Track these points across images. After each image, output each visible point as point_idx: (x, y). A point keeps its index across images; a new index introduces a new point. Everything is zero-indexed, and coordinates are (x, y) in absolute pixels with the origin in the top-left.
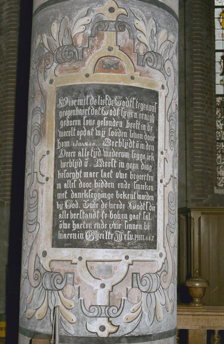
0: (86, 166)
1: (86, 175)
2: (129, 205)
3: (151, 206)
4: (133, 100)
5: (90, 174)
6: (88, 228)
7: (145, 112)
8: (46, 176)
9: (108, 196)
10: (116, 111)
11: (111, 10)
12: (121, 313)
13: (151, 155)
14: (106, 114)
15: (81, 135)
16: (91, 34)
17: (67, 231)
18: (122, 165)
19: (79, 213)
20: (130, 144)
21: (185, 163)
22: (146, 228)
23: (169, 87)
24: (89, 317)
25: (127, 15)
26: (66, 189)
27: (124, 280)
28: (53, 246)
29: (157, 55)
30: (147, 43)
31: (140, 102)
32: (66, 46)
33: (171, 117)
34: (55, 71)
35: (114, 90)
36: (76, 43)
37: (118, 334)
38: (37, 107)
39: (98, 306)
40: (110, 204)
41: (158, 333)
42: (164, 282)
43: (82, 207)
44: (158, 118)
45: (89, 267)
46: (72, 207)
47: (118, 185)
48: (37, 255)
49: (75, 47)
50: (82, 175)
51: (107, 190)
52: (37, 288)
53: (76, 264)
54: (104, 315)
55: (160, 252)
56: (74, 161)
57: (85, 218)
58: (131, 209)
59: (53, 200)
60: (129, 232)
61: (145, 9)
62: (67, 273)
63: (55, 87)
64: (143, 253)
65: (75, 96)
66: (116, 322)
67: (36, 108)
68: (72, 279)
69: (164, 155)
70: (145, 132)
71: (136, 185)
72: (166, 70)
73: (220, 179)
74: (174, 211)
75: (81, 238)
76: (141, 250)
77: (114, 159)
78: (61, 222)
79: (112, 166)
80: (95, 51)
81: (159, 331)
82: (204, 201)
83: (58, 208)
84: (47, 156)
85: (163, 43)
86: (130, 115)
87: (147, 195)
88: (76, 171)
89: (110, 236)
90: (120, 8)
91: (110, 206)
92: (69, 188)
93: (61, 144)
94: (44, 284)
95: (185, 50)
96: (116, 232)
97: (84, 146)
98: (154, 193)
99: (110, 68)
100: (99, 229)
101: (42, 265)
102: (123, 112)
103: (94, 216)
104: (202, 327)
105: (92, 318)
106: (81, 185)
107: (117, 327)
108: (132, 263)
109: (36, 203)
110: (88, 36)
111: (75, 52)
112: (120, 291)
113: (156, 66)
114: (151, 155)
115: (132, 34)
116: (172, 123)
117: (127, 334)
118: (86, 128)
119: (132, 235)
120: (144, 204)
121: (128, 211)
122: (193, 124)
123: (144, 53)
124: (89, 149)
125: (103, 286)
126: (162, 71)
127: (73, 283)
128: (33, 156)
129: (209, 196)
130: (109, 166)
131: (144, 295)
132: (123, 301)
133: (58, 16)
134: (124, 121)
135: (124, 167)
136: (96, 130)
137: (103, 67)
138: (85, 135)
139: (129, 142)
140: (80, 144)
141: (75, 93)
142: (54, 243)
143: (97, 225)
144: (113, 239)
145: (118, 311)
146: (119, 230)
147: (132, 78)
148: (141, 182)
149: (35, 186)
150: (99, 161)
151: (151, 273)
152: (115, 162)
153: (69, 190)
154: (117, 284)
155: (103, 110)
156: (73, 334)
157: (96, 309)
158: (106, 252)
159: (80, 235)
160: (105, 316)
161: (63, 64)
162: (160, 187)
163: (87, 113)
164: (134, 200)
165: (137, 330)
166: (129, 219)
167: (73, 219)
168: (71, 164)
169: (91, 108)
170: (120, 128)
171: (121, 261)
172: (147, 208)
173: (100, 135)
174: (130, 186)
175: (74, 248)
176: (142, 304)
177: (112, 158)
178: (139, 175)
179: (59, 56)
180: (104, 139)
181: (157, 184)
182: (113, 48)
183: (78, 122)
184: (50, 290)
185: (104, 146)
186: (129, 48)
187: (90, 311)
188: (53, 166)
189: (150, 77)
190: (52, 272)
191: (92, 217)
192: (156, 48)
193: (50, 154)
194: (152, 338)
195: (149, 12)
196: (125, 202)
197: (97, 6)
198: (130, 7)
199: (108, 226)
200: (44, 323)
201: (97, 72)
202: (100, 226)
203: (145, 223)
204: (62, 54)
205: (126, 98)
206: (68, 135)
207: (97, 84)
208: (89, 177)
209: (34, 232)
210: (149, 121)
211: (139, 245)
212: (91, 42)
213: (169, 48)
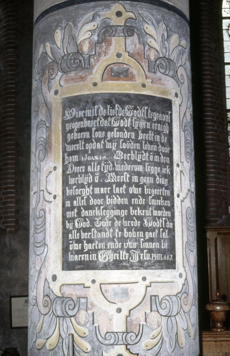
0: (97, 181)
1: (97, 190)
2: (144, 222)
3: (168, 223)
4: (145, 110)
6: (101, 247)
7: (159, 122)
8: (54, 193)
9: (122, 213)
10: (128, 121)
11: (119, 14)
13: (166, 168)
14: (116, 125)
15: (90, 148)
16: (98, 40)
17: (78, 252)
18: (135, 179)
19: (91, 232)
20: (144, 156)
23: (183, 95)
25: (135, 18)
26: (76, 207)
28: (63, 269)
29: (169, 60)
30: (158, 49)
31: (153, 111)
32: (72, 54)
33: (186, 128)
35: (124, 99)
36: (82, 50)
38: (42, 121)
39: (114, 332)
40: (124, 221)
42: (185, 305)
43: (93, 225)
45: (103, 290)
46: (83, 226)
48: (46, 279)
50: (93, 191)
51: (120, 207)
52: (47, 316)
53: (89, 287)
54: (122, 343)
56: (83, 176)
57: (97, 237)
58: (147, 226)
59: (62, 220)
61: (154, 12)
62: (80, 298)
63: (60, 98)
64: (161, 274)
65: (82, 107)
67: (40, 122)
68: (85, 304)
69: (180, 168)
71: (151, 200)
72: (179, 77)
74: (193, 228)
75: (93, 259)
76: (160, 271)
77: (126, 173)
79: (125, 181)
80: (103, 58)
82: (218, 222)
83: (67, 228)
84: (54, 172)
85: (174, 48)
86: (143, 126)
87: (163, 211)
88: (87, 187)
89: (125, 256)
90: (128, 11)
91: (124, 223)
93: (69, 158)
94: (54, 311)
96: (132, 252)
97: (93, 159)
98: (171, 209)
99: (119, 76)
101: (52, 291)
103: (108, 234)
105: (109, 346)
106: (92, 202)
108: (150, 285)
109: (43, 224)
110: (94, 42)
111: (82, 60)
112: (138, 316)
113: (169, 73)
114: (166, 168)
115: (141, 39)
116: (187, 134)
119: (149, 255)
120: (161, 220)
121: (143, 229)
123: (155, 59)
124: (99, 163)
125: (119, 310)
127: (87, 309)
129: (224, 216)
130: (122, 181)
131: (164, 319)
132: (141, 326)
133: (61, 23)
135: (137, 181)
136: (107, 142)
137: (112, 75)
138: (94, 148)
139: (142, 154)
140: (89, 158)
141: (82, 104)
143: (110, 245)
144: (129, 259)
145: (136, 337)
147: (144, 86)
148: (157, 197)
149: (42, 205)
150: (111, 175)
151: (170, 295)
153: (79, 208)
154: (134, 308)
155: (113, 121)
157: (113, 336)
158: (122, 273)
160: (123, 343)
161: (69, 73)
162: (177, 202)
163: (96, 124)
164: (150, 216)
167: (84, 239)
168: (81, 180)
169: (101, 119)
170: (132, 140)
171: (137, 283)
172: (164, 224)
173: (111, 147)
174: (145, 201)
175: (87, 270)
176: (163, 330)
177: (124, 171)
178: (154, 189)
179: (64, 65)
180: (115, 152)
181: (173, 199)
182: (121, 54)
183: (87, 135)
184: (62, 317)
185: (115, 160)
186: (138, 54)
187: (105, 338)
189: (162, 84)
190: (63, 297)
191: (105, 236)
192: (167, 54)
193: (57, 170)
195: (159, 15)
196: (140, 218)
197: (103, 10)
198: (139, 10)
199: (122, 245)
201: (106, 80)
202: (114, 245)
203: (162, 241)
204: (67, 63)
205: (138, 107)
206: (76, 148)
207: (106, 93)
208: (100, 193)
209: (42, 255)
210: (163, 131)
211: (157, 265)
212: (98, 49)
213: (181, 53)
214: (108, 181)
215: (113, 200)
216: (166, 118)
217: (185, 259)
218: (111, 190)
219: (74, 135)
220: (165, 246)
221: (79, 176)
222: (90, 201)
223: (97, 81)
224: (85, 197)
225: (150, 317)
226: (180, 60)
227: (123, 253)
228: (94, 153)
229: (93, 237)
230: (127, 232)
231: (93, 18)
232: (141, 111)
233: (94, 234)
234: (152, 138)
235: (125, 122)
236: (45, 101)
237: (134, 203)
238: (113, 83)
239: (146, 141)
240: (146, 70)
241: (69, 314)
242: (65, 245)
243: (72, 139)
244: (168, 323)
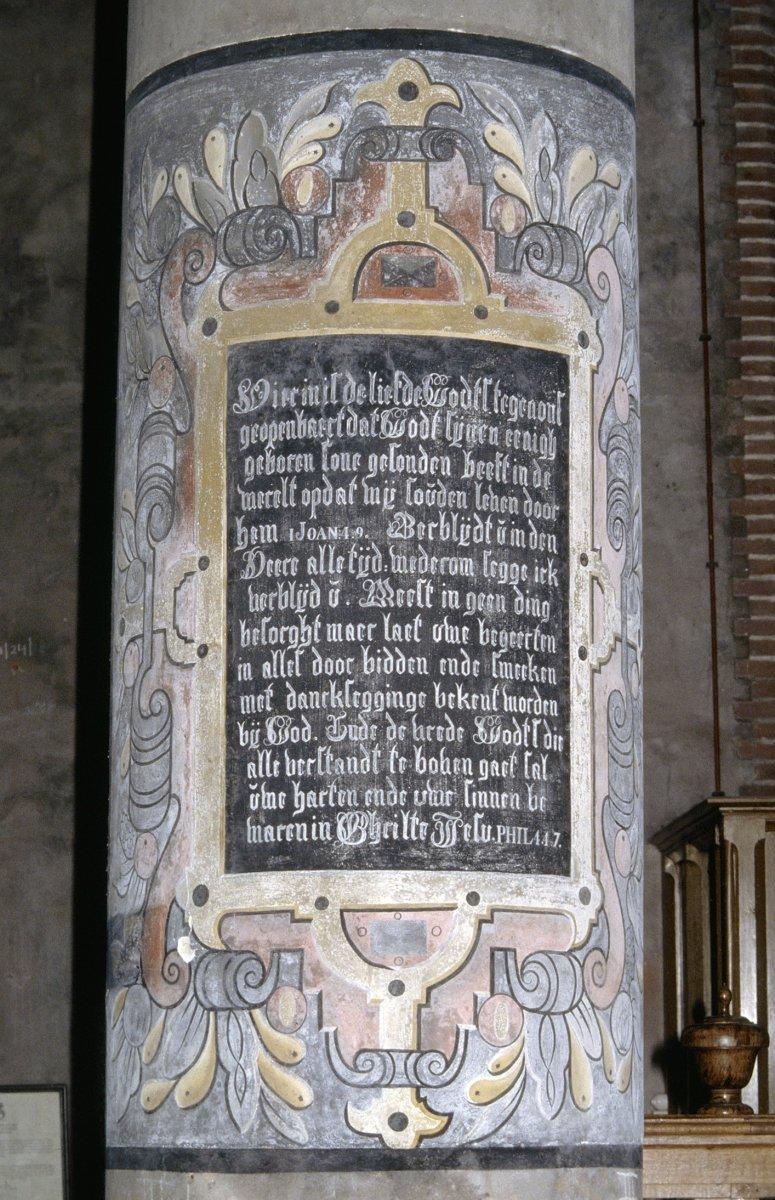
0: (334, 604)
1: (334, 632)
2: (476, 730)
3: (549, 734)
4: (485, 388)
5: (348, 632)
6: (346, 803)
7: (525, 424)
9: (408, 702)
11: (408, 91)
12: (456, 1075)
13: (546, 566)
14: (396, 432)
15: (314, 504)
16: (343, 172)
18: (451, 598)
19: (314, 756)
20: (478, 530)
21: (708, 627)
22: (533, 804)
23: (604, 339)
26: (270, 681)
27: (463, 972)
28: (228, 868)
30: (527, 197)
31: (508, 391)
32: (260, 211)
33: (614, 440)
35: (421, 354)
36: (292, 199)
38: (160, 412)
39: (382, 1051)
41: (577, 1144)
43: (323, 735)
44: (567, 444)
45: (350, 930)
46: (290, 739)
47: (439, 664)
49: (289, 213)
50: (322, 633)
51: (403, 683)
52: (178, 1008)
53: (309, 920)
54: (404, 1081)
55: (581, 886)
56: (292, 587)
57: (333, 772)
59: (227, 720)
60: (478, 816)
61: (518, 83)
62: (279, 951)
64: (525, 886)
65: (292, 376)
67: (155, 414)
68: (297, 971)
69: (590, 567)
70: (525, 491)
72: (594, 280)
74: (630, 757)
75: (323, 838)
77: (424, 581)
78: (253, 787)
79: (420, 604)
80: (356, 227)
81: (581, 1139)
83: (242, 744)
84: (199, 574)
87: (536, 698)
88: (303, 621)
89: (417, 828)
90: (436, 83)
91: (415, 731)
92: (280, 677)
93: (249, 533)
94: (200, 994)
95: (699, 124)
96: (437, 817)
97: (324, 538)
98: (559, 691)
100: (380, 806)
101: (193, 933)
102: (452, 426)
103: (366, 765)
105: (364, 1091)
108: (489, 918)
109: (164, 733)
110: (331, 176)
111: (291, 231)
112: (454, 1005)
115: (476, 169)
116: (617, 461)
117: (478, 1140)
118: (333, 480)
119: (490, 827)
121: (472, 750)
122: (742, 453)
123: (517, 228)
124: (342, 549)
125: (397, 988)
127: (301, 983)
128: (149, 577)
130: (410, 605)
131: (531, 1022)
133: (228, 109)
134: (457, 455)
135: (458, 607)
136: (365, 486)
138: (328, 504)
139: (474, 523)
140: (312, 534)
141: (293, 367)
144: (428, 837)
145: (448, 1065)
147: (481, 313)
148: (516, 656)
151: (551, 952)
152: (430, 589)
153: (279, 685)
154: (442, 982)
156: (303, 1143)
157: (377, 1060)
158: (405, 880)
159: (318, 828)
161: (251, 268)
162: (579, 672)
163: (334, 430)
164: (493, 712)
165: (508, 1130)
166: (476, 775)
167: (295, 778)
168: (285, 599)
170: (444, 480)
173: (378, 502)
174: (481, 668)
176: (525, 1050)
177: (418, 576)
178: (509, 632)
180: (391, 516)
181: (567, 662)
182: (414, 216)
183: (305, 462)
185: (391, 539)
186: (466, 215)
188: (223, 605)
189: (539, 307)
191: (359, 769)
193: (210, 567)
194: (559, 1158)
195: (532, 93)
196: (464, 718)
199: (410, 797)
200: (206, 1114)
201: (366, 295)
202: (385, 796)
203: (530, 789)
204: (244, 237)
206: (271, 503)
207: (366, 336)
208: (345, 641)
210: (540, 455)
212: (342, 198)
213: (603, 205)
216: (549, 412)
217: (601, 850)
218: (378, 632)
219: (264, 461)
220: (538, 803)
221: (280, 587)
222: (314, 663)
223: (338, 298)
224: (298, 653)
225: (488, 1011)
226: (596, 228)
228: (325, 518)
229: (320, 773)
230: (423, 759)
231: (328, 101)
232: (473, 390)
234: (504, 476)
236: (171, 351)
237: (447, 672)
238: (387, 305)
239: (485, 482)
240: (490, 265)
241: (247, 999)
242: (236, 797)
243: (259, 473)
244: (543, 1031)
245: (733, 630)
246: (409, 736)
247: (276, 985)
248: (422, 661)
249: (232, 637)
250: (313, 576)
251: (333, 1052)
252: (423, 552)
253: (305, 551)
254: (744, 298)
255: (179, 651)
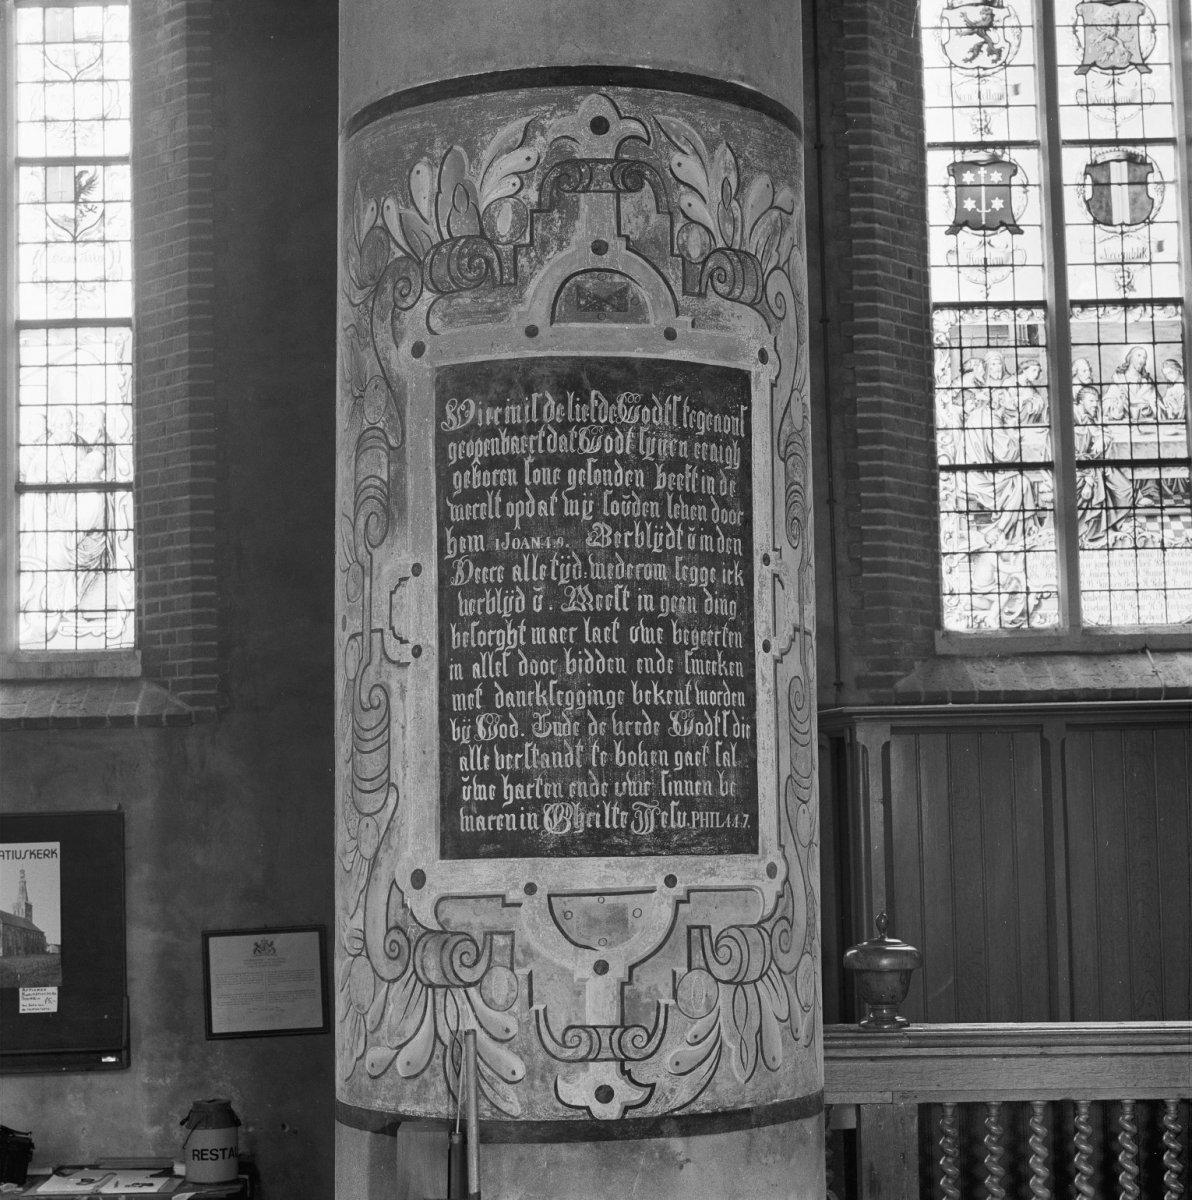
1: (538, 636)
5: (551, 635)
6: (551, 795)
7: (712, 437)
8: (413, 640)
10: (625, 439)
11: (599, 126)
12: (657, 1048)
13: (732, 569)
14: (592, 448)
15: (518, 516)
16: (539, 203)
17: (486, 808)
18: (646, 602)
19: (522, 751)
22: (724, 790)
23: (781, 355)
24: (562, 1060)
25: (646, 138)
27: (662, 951)
28: (443, 855)
30: (712, 225)
32: (463, 241)
34: (428, 317)
35: (615, 374)
36: (493, 230)
37: (650, 1110)
40: (614, 721)
42: (782, 951)
43: (529, 732)
44: (750, 454)
48: (394, 882)
50: (527, 636)
51: (603, 682)
53: (519, 905)
55: (769, 861)
56: (499, 595)
57: (539, 766)
59: (440, 717)
60: (673, 804)
61: (701, 116)
62: (492, 933)
63: (429, 367)
64: (718, 866)
66: (644, 1073)
67: (368, 430)
68: (508, 952)
69: (772, 566)
70: (713, 499)
71: (690, 661)
72: (772, 301)
73: (954, 600)
74: (808, 736)
76: (713, 857)
78: (465, 780)
80: (554, 256)
81: (772, 1099)
84: (413, 580)
86: (668, 450)
87: (725, 691)
88: (509, 626)
89: (618, 816)
90: (625, 118)
91: (615, 727)
92: (489, 677)
93: (458, 543)
94: (419, 970)
96: (636, 806)
98: (746, 684)
99: (601, 309)
102: (645, 441)
103: (570, 759)
104: (904, 1096)
105: (573, 1065)
106: (525, 666)
107: (648, 1090)
109: (383, 725)
112: (654, 983)
113: (742, 293)
114: (732, 569)
119: (685, 814)
121: (669, 743)
122: (855, 412)
123: (702, 254)
124: (545, 558)
125: (601, 968)
126: (758, 307)
127: (512, 964)
130: (608, 609)
131: (726, 991)
132: (663, 1010)
133: (431, 144)
137: (579, 306)
138: (530, 516)
139: (666, 531)
140: (517, 544)
142: (448, 845)
143: (577, 787)
145: (649, 1040)
146: (645, 799)
147: (670, 335)
148: (706, 653)
149: (379, 673)
151: (742, 926)
152: (626, 593)
153: (488, 685)
154: (644, 960)
155: (582, 437)
157: (584, 1036)
158: (608, 866)
159: (526, 818)
160: (611, 1056)
162: (763, 663)
164: (686, 706)
165: (706, 1097)
167: (504, 771)
168: (493, 604)
169: (548, 432)
170: (638, 491)
173: (577, 514)
174: (674, 665)
175: (511, 857)
176: (721, 1019)
178: (699, 631)
180: (589, 525)
182: (607, 245)
183: (509, 476)
184: (440, 986)
185: (591, 548)
186: (655, 242)
187: (564, 1042)
188: (435, 609)
190: (444, 932)
191: (563, 763)
192: (738, 238)
194: (753, 1119)
195: (714, 125)
196: (660, 713)
198: (656, 113)
199: (611, 789)
200: (426, 1085)
201: (563, 320)
202: (588, 789)
203: (721, 776)
205: (654, 397)
206: (478, 514)
207: (564, 358)
209: (379, 815)
212: (540, 228)
213: (779, 230)
214: (570, 609)
215: (583, 663)
216: (731, 425)
217: (785, 825)
218: (579, 635)
219: (471, 476)
220: (729, 788)
222: (520, 664)
227: (611, 811)
228: (528, 528)
231: (525, 135)
232: (664, 407)
233: (533, 757)
234: (693, 486)
235: (617, 439)
236: (383, 371)
237: (644, 670)
238: (583, 329)
240: (678, 288)
241: (462, 977)
242: (449, 788)
243: (466, 487)
245: (849, 552)
246: (609, 731)
247: (489, 965)
248: (621, 661)
249: (444, 638)
250: (518, 583)
251: (543, 1029)
252: (620, 559)
253: (511, 559)
254: (856, 287)
255: (395, 650)
